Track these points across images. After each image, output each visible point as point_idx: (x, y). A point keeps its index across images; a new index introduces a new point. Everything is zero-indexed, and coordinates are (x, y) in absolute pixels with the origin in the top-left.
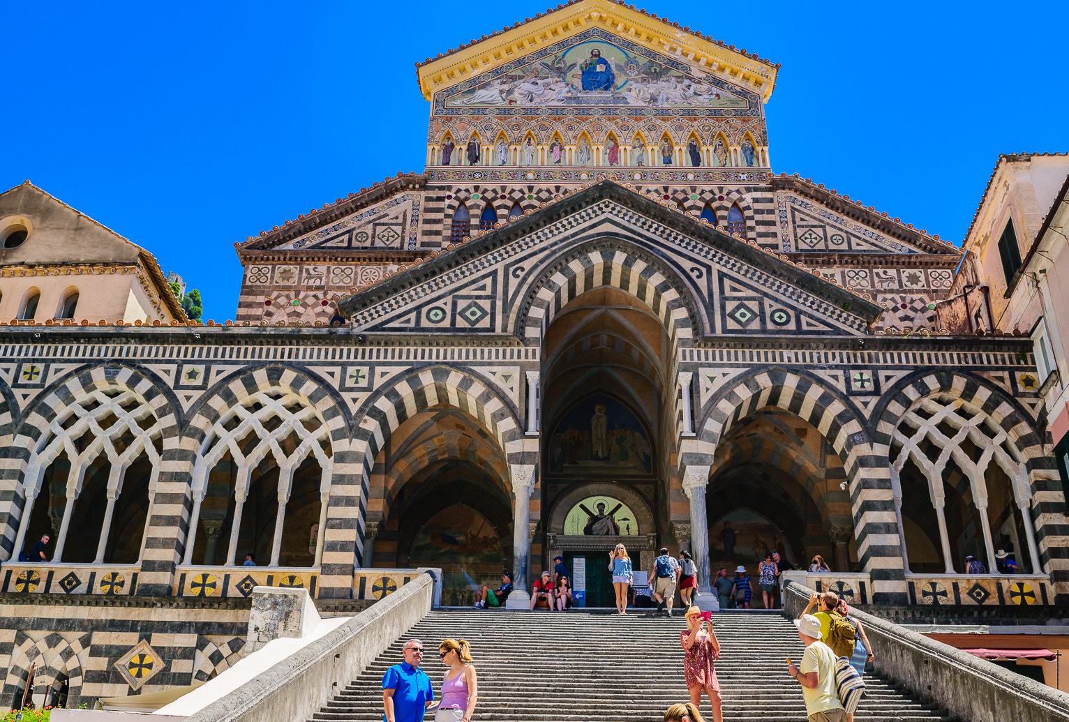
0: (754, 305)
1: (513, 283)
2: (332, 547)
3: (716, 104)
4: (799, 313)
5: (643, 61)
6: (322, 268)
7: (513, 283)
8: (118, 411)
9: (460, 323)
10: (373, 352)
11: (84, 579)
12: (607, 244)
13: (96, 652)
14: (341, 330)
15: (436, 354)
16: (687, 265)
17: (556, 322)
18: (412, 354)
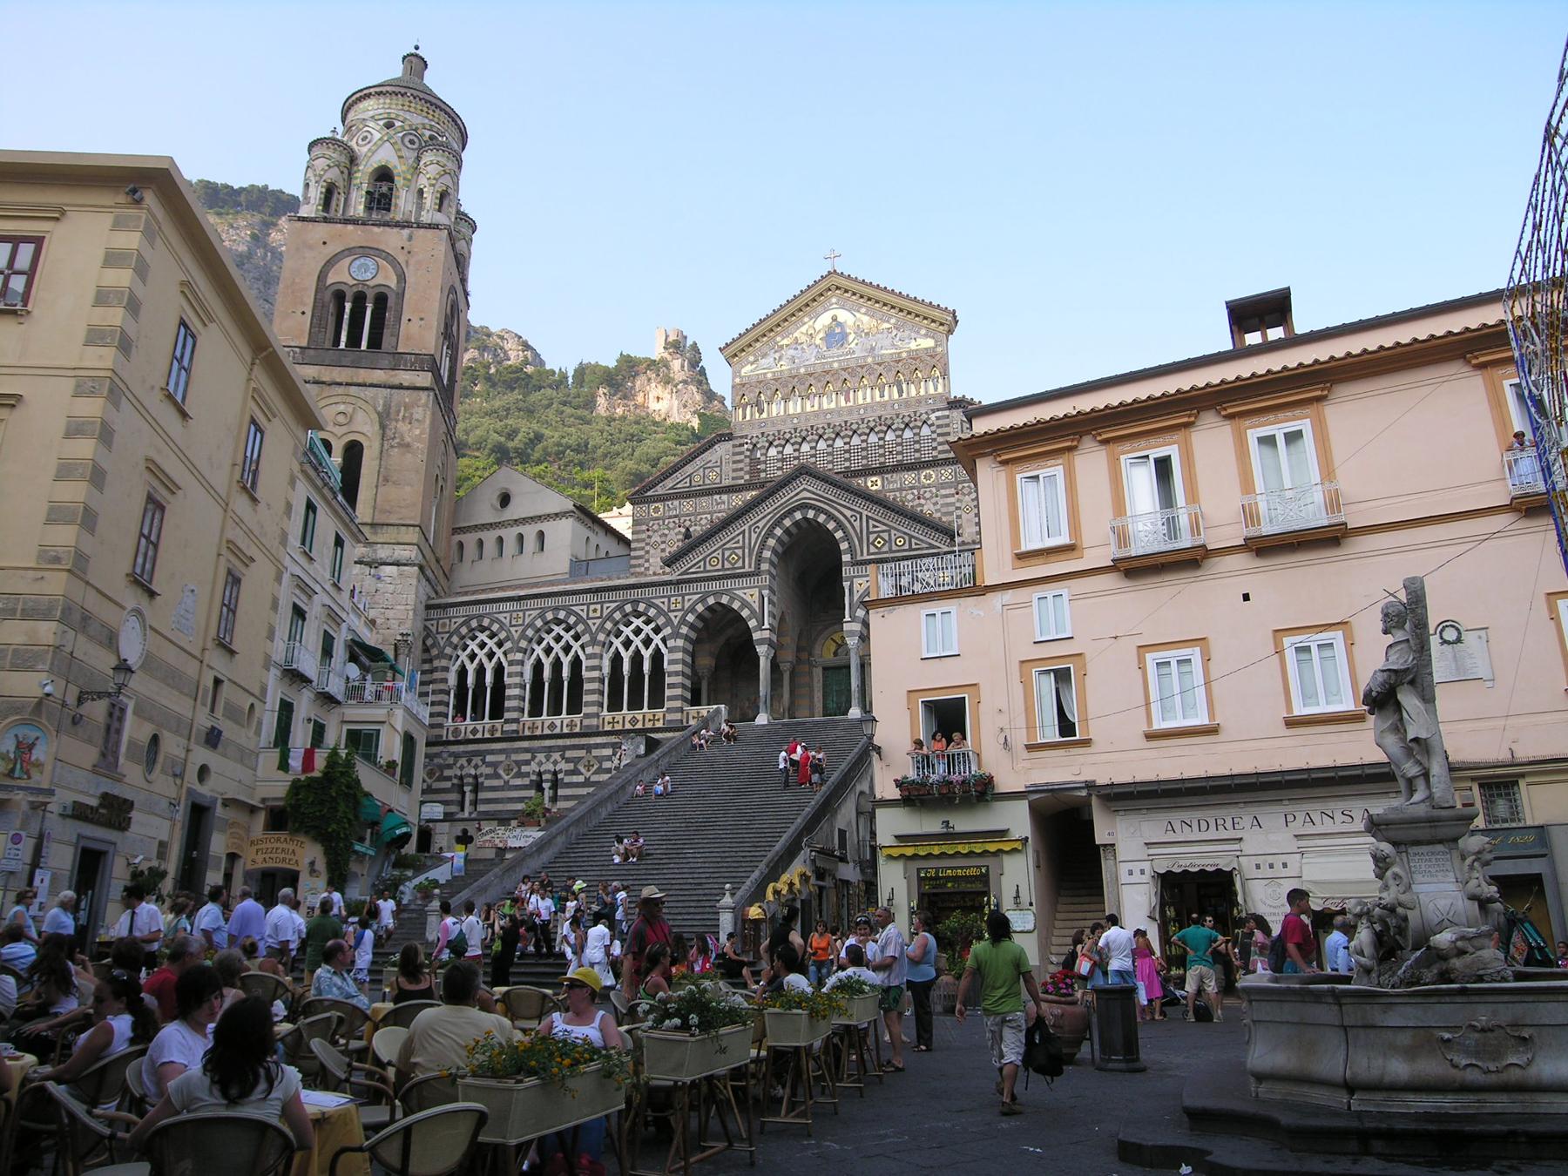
0: (885, 536)
1: (754, 536)
2: (670, 698)
3: (913, 345)
4: (911, 537)
5: (866, 319)
6: (676, 503)
7: (754, 536)
8: (562, 633)
9: (727, 565)
10: (685, 589)
11: (558, 723)
12: (804, 507)
13: (568, 761)
14: (666, 578)
15: (715, 586)
16: (848, 513)
17: (784, 553)
18: (703, 587)
